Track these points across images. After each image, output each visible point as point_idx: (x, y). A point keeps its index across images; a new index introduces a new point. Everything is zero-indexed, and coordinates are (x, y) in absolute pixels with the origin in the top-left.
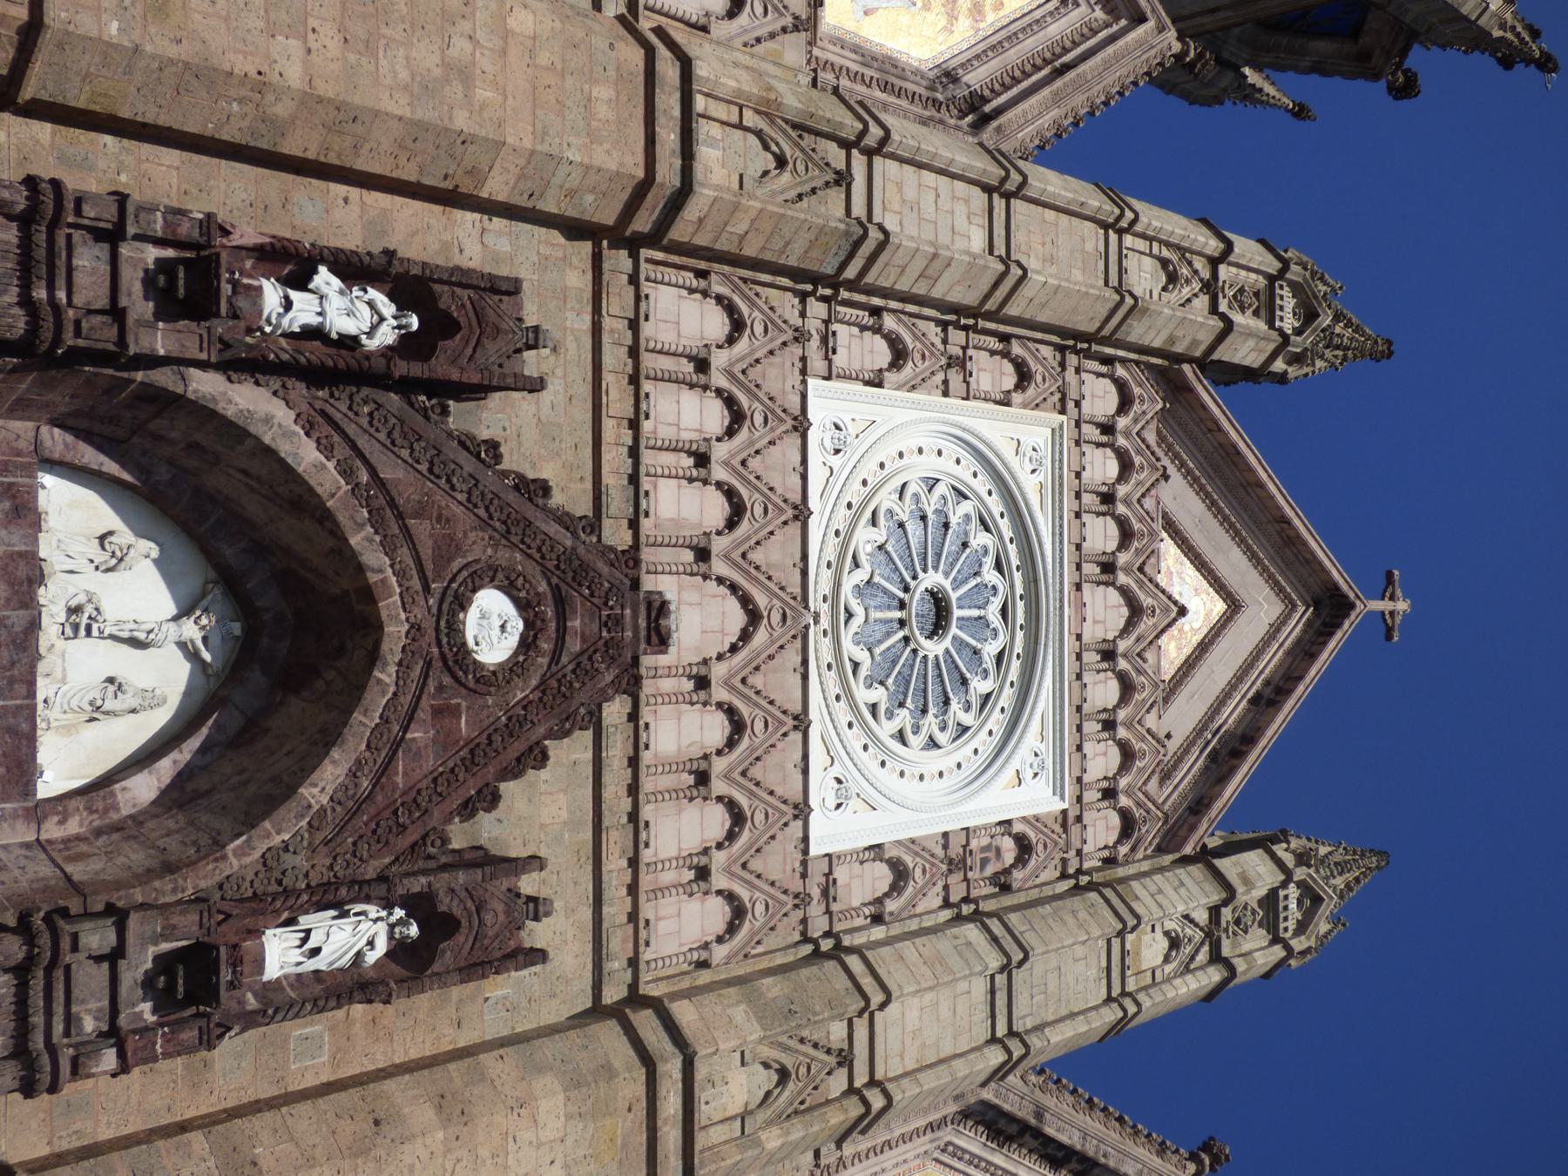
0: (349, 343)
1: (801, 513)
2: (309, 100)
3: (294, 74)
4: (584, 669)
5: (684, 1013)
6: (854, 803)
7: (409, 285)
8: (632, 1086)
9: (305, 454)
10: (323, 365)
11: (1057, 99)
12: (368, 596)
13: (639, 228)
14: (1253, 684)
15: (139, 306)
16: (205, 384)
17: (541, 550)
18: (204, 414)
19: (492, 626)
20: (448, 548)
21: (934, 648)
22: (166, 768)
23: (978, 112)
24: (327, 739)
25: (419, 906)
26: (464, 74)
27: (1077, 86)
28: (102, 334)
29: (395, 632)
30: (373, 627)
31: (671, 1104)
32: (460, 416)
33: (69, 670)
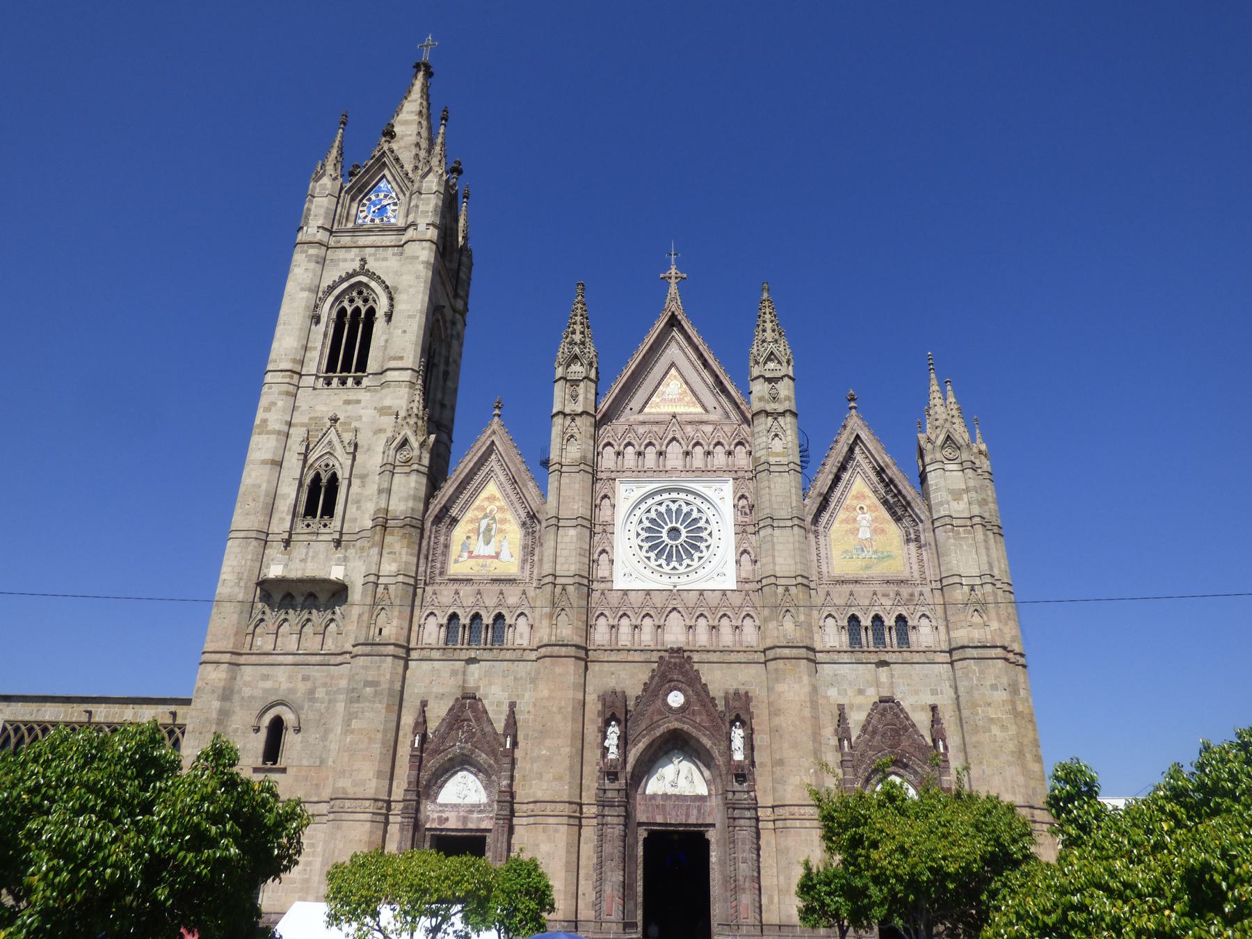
0: (619, 738)
2: (572, 745)
3: (568, 749)
4: (685, 674)
5: (769, 643)
6: (724, 571)
9: (641, 746)
10: (624, 742)
11: (525, 485)
12: (669, 731)
13: (584, 655)
15: (616, 785)
16: (629, 768)
17: (659, 687)
18: (635, 767)
19: (676, 699)
20: (660, 712)
21: (683, 531)
22: (703, 769)
23: (532, 516)
24: (698, 740)
25: (732, 723)
26: (560, 708)
27: (520, 476)
28: (623, 793)
29: (677, 725)
30: (675, 730)
31: (787, 652)
32: (631, 704)
33: (684, 788)
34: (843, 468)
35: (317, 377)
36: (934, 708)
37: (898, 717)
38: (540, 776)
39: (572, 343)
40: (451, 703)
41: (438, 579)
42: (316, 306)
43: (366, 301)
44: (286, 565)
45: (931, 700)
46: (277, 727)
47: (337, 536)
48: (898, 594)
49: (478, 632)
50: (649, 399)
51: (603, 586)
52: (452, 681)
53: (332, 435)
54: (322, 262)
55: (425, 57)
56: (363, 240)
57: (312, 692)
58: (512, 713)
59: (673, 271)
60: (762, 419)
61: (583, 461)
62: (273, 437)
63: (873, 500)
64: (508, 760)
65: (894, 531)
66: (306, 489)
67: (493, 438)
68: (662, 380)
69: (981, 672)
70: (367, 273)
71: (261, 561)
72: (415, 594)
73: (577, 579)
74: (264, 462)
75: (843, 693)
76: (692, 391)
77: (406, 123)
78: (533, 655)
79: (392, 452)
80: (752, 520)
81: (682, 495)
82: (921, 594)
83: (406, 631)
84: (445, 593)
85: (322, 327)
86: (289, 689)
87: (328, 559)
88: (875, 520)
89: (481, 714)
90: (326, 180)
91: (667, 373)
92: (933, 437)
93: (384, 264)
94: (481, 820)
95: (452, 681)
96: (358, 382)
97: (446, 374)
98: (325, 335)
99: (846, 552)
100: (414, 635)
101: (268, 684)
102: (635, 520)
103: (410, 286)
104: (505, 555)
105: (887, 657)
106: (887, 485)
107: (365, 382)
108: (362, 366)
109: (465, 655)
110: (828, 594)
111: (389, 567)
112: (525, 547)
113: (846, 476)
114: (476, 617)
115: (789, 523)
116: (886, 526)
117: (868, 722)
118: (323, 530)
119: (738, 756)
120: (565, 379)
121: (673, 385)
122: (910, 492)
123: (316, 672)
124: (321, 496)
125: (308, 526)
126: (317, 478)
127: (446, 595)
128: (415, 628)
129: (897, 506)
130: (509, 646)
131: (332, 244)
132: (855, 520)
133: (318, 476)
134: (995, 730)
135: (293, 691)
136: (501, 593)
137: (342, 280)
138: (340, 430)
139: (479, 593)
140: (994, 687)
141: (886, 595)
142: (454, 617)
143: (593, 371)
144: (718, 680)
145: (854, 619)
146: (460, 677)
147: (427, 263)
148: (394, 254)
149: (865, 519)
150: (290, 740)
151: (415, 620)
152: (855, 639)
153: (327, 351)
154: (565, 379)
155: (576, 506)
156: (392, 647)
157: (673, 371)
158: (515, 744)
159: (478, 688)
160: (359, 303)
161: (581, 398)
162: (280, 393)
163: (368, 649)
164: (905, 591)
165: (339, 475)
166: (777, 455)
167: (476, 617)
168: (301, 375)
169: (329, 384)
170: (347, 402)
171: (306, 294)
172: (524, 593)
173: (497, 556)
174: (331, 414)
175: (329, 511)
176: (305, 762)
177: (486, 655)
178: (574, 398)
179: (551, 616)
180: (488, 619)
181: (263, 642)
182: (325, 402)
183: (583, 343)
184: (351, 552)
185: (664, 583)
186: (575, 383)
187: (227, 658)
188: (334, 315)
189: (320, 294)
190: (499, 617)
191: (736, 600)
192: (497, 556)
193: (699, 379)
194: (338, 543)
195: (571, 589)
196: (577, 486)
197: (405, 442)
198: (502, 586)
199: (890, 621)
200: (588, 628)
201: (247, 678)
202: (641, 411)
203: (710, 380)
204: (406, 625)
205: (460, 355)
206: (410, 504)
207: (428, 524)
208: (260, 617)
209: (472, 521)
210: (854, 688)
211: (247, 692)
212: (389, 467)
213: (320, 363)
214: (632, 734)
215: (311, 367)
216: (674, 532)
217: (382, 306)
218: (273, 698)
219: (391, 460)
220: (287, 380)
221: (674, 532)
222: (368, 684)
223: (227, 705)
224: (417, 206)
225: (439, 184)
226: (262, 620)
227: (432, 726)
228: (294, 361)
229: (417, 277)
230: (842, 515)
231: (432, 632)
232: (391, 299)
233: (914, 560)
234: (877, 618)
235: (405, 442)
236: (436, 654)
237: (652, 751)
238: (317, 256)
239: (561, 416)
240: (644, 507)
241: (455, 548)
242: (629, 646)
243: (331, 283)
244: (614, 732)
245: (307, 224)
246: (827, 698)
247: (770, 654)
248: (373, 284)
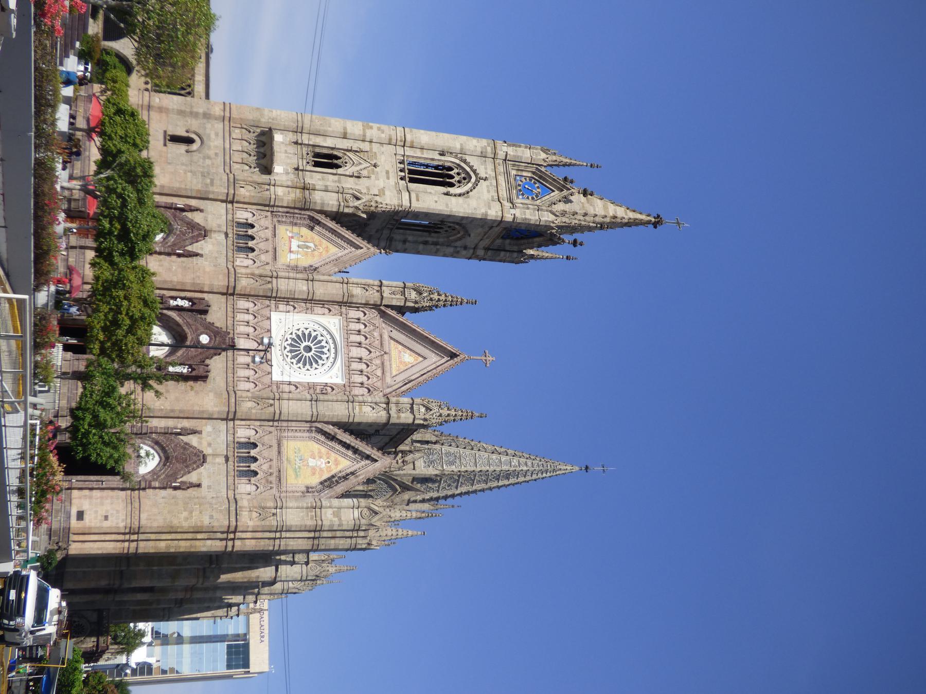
1: (269, 331)
7: (190, 300)
8: (225, 395)
9: (178, 319)
10: (179, 309)
13: (230, 293)
14: (425, 371)
16: (165, 312)
18: (165, 315)
19: (204, 339)
21: (310, 354)
25: (190, 366)
30: (186, 338)
34: (356, 451)
35: (403, 156)
36: (199, 486)
37: (195, 462)
38: (162, 266)
39: (431, 292)
41: (275, 220)
42: (451, 153)
43: (459, 182)
45: (204, 485)
46: (189, 141)
47: (301, 168)
48: (271, 474)
49: (243, 239)
50: (400, 343)
51: (273, 306)
53: (365, 165)
54: (483, 155)
56: (501, 179)
57: (209, 158)
58: (197, 255)
59: (491, 358)
60: (384, 400)
61: (351, 296)
62: (361, 133)
64: (169, 250)
65: (314, 481)
66: (330, 152)
68: (414, 352)
69: (221, 511)
71: (284, 130)
72: (265, 205)
73: (275, 289)
74: (345, 128)
75: (209, 434)
77: (605, 208)
78: (230, 267)
79: (351, 191)
80: (318, 392)
81: (333, 355)
82: (271, 488)
83: (242, 200)
85: (438, 157)
87: (287, 164)
88: (321, 470)
89: (195, 240)
90: (543, 156)
91: (419, 355)
96: (402, 179)
97: (426, 243)
98: (433, 159)
99: (299, 449)
100: (241, 205)
101: (213, 136)
102: (316, 327)
104: (293, 256)
105: (230, 463)
106: (344, 477)
108: (412, 180)
109: (230, 231)
110: (270, 432)
111: (280, 191)
113: (350, 453)
114: (253, 238)
115: (314, 410)
116: (317, 476)
117: (191, 447)
119: (171, 369)
120: (404, 288)
121: (408, 358)
122: (341, 488)
123: (220, 159)
124: (327, 160)
127: (267, 222)
128: (245, 206)
129: (329, 482)
131: (497, 161)
132: (321, 457)
133: (340, 158)
134: (185, 514)
135: (209, 148)
136: (267, 252)
137: (471, 167)
139: (267, 240)
140: (211, 517)
141: (270, 467)
142: (252, 226)
143: (412, 305)
144: (217, 364)
145: (255, 445)
146: (217, 229)
147: (486, 215)
148: (492, 197)
149: (322, 463)
150: (182, 148)
151: (250, 206)
152: (242, 445)
153: (422, 161)
154: (404, 288)
155: (321, 291)
157: (421, 359)
158: (179, 255)
160: (457, 178)
162: (390, 135)
163: (232, 180)
164: (273, 479)
166: (360, 409)
167: (253, 238)
168: (404, 146)
169: (402, 162)
170: (387, 172)
171: (458, 146)
172: (268, 264)
173: (291, 252)
174: (379, 163)
175: (317, 164)
176: (169, 155)
177: (230, 242)
178: (393, 293)
179: (253, 274)
180: (251, 244)
181: (237, 133)
182: (387, 160)
183: (431, 300)
185: (276, 340)
186: (403, 293)
187: (227, 114)
188: (447, 164)
189: (459, 156)
190: (253, 250)
191: (266, 380)
192: (291, 252)
194: (297, 169)
195: (270, 286)
196: (334, 292)
197: (358, 199)
198: (271, 253)
199: (254, 467)
200: (246, 296)
201: (216, 125)
202: (391, 338)
204: (246, 200)
205: (445, 255)
206: (319, 201)
207: (308, 213)
209: (313, 238)
210: (212, 439)
211: (209, 126)
212: (341, 190)
213: (413, 157)
214: (184, 314)
215: (409, 152)
216: (308, 349)
217: (452, 190)
218: (205, 139)
219: (346, 191)
220: (399, 139)
221: (308, 349)
223: (201, 116)
224: (528, 208)
225: (546, 221)
227: (189, 215)
228: (412, 142)
230: (323, 450)
231: (243, 215)
232: (460, 195)
234: (255, 460)
235: (358, 199)
236: (230, 217)
237: (175, 327)
238: (486, 152)
239: (379, 284)
240: (325, 333)
241: (296, 229)
242: (237, 319)
243: (468, 160)
244: (186, 304)
245: (509, 145)
246: (206, 425)
247: (232, 393)
248: (470, 185)
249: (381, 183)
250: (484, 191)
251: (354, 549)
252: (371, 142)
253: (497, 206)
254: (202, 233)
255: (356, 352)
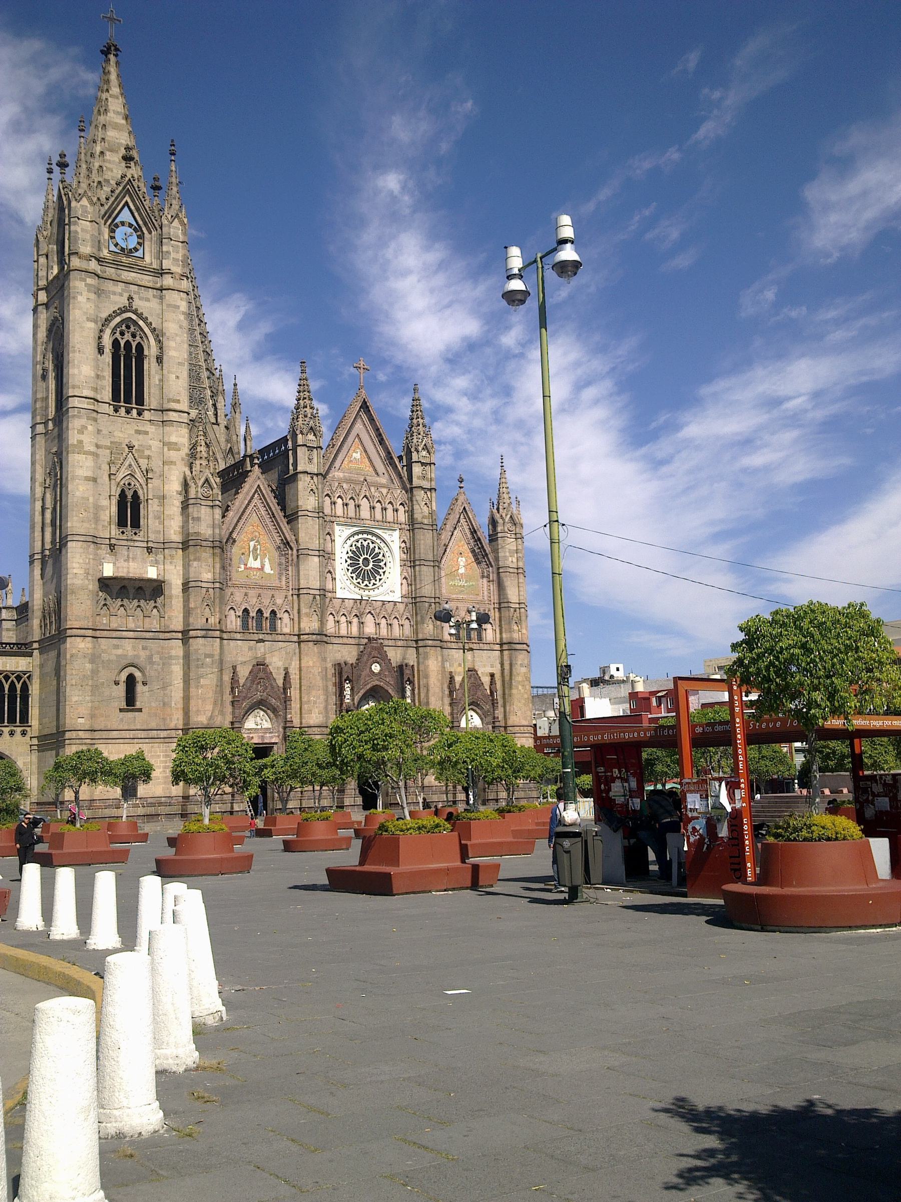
5: (420, 636)
9: (360, 694)
29: (377, 683)
40: (251, 668)
42: (100, 338)
43: (134, 336)
44: (114, 564)
46: (131, 681)
49: (259, 623)
52: (250, 654)
54: (99, 292)
55: (112, 33)
57: (150, 657)
63: (466, 549)
65: (476, 570)
67: (258, 482)
70: (135, 312)
76: (369, 458)
81: (370, 537)
84: (238, 594)
86: (135, 656)
89: (269, 676)
92: (504, 515)
93: (147, 304)
94: (272, 737)
95: (250, 654)
101: (120, 652)
103: (177, 335)
104: (268, 569)
105: (471, 646)
106: (476, 541)
107: (147, 415)
108: (140, 401)
109: (256, 637)
112: (280, 564)
114: (260, 612)
118: (136, 538)
124: (129, 511)
125: (123, 533)
126: (123, 495)
130: (279, 632)
133: (123, 491)
137: (116, 313)
138: (136, 455)
140: (521, 665)
148: (154, 296)
149: (462, 561)
150: (139, 688)
156: (218, 632)
159: (265, 658)
160: (128, 336)
161: (315, 460)
165: (140, 493)
167: (260, 612)
170: (138, 432)
171: (92, 325)
174: (127, 441)
176: (153, 704)
177: (267, 637)
178: (310, 460)
180: (267, 614)
184: (160, 557)
187: (90, 633)
190: (273, 612)
191: (401, 607)
192: (262, 569)
193: (375, 451)
201: (103, 647)
203: (383, 454)
208: (103, 603)
211: (105, 657)
218: (125, 662)
220: (92, 407)
222: (207, 656)
226: (105, 605)
229: (181, 327)
231: (233, 622)
233: (485, 589)
236: (238, 636)
247: (421, 643)
248: (141, 323)
249: (155, 444)
250: (147, 305)
251: (551, 543)
252: (98, 446)
253: (172, 297)
254: (260, 666)
255: (365, 513)
